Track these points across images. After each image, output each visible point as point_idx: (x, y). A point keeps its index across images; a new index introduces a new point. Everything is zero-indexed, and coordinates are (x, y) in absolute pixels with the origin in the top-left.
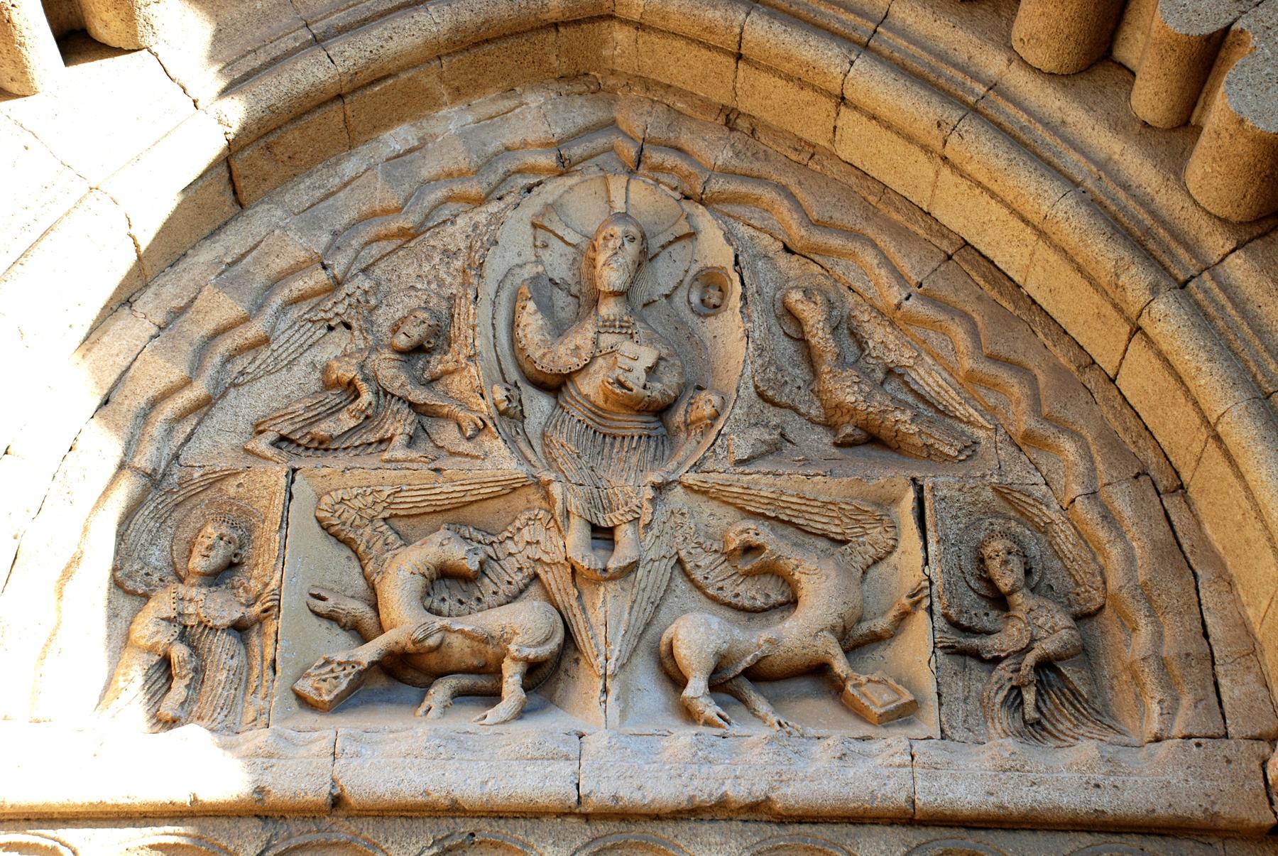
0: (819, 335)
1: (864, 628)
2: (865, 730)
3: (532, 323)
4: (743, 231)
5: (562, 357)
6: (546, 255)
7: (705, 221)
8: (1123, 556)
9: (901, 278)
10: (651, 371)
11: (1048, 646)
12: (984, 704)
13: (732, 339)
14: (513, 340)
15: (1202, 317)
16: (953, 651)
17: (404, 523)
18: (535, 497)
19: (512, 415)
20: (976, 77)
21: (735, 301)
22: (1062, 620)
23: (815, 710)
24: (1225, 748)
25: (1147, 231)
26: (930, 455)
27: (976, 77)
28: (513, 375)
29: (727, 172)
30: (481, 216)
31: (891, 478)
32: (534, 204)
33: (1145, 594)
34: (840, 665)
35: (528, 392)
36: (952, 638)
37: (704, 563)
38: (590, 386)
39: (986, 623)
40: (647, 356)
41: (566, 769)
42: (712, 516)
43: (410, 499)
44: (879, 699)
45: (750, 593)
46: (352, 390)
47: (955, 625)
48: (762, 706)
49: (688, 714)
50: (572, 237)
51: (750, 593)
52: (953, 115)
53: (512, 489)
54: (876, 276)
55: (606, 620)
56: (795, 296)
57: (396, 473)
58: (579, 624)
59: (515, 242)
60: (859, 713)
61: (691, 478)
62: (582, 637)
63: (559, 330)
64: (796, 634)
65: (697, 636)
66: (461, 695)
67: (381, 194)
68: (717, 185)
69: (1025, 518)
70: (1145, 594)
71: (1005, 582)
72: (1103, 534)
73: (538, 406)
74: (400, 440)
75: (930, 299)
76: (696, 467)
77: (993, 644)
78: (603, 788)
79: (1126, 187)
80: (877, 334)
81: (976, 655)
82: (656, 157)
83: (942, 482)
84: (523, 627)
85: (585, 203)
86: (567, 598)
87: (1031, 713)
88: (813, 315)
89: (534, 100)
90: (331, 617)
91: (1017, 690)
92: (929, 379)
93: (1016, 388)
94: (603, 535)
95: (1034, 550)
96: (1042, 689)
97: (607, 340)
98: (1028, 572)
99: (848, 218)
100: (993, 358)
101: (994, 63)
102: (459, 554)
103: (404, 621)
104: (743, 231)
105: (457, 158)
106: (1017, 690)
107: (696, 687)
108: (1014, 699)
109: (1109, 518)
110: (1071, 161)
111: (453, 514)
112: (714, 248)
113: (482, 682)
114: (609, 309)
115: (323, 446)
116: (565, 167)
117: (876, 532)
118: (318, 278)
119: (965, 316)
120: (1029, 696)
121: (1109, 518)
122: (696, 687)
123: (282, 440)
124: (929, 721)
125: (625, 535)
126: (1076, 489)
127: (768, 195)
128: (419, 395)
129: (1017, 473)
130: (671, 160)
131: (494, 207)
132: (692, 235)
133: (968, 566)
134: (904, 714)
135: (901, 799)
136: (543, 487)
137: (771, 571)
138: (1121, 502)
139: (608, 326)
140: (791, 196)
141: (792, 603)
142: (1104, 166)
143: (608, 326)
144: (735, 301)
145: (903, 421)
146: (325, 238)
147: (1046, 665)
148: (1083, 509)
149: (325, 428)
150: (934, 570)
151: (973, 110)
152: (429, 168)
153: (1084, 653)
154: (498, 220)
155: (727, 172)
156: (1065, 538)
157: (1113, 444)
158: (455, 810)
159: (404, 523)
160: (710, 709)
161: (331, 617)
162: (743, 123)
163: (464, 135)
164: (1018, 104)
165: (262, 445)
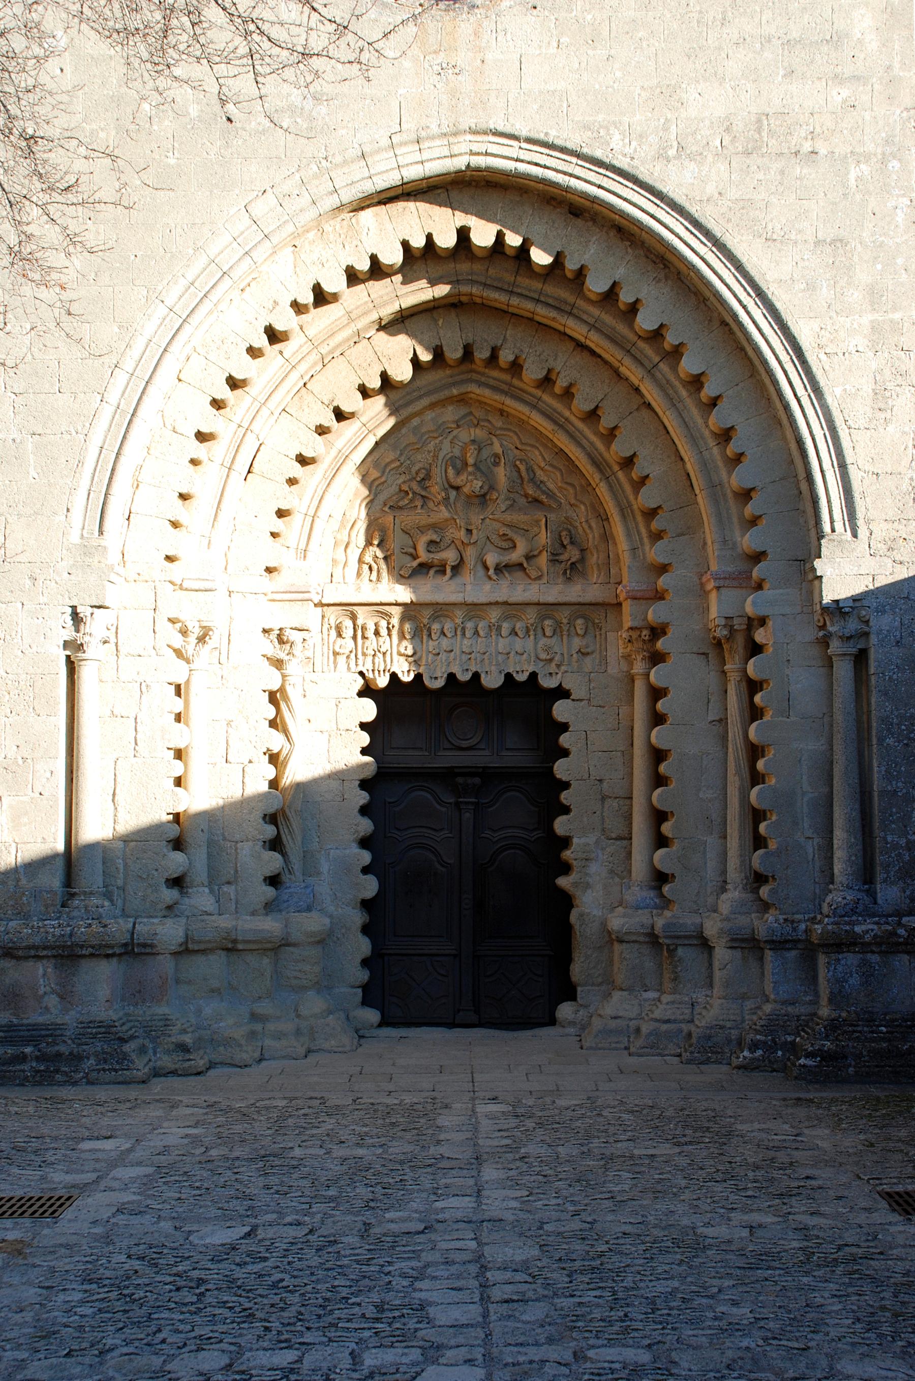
0: (524, 474)
1: (531, 554)
2: (530, 581)
3: (451, 471)
4: (505, 443)
5: (458, 482)
6: (454, 450)
7: (495, 440)
8: (592, 537)
9: (544, 459)
10: (481, 487)
11: (573, 560)
12: (558, 573)
13: (502, 474)
14: (446, 476)
15: (611, 487)
16: (551, 561)
17: (422, 529)
18: (453, 522)
19: (447, 499)
20: (562, 416)
21: (502, 464)
22: (577, 553)
23: (520, 574)
24: (609, 586)
25: (601, 463)
26: (549, 508)
27: (562, 416)
28: (447, 486)
29: (501, 429)
30: (437, 441)
31: (540, 515)
32: (450, 437)
33: (596, 547)
34: (525, 565)
35: (450, 490)
36: (551, 558)
37: (494, 537)
38: (466, 490)
39: (560, 551)
40: (480, 484)
41: (462, 595)
42: (497, 525)
43: (423, 523)
44: (534, 574)
45: (505, 545)
46: (407, 493)
47: (552, 554)
48: (507, 575)
49: (490, 578)
50: (460, 444)
51: (505, 545)
52: (556, 428)
53: (447, 520)
54: (537, 457)
55: (470, 554)
56: (518, 463)
57: (418, 517)
58: (464, 555)
59: (446, 447)
60: (530, 577)
61: (491, 517)
62: (465, 558)
63: (458, 473)
64: (516, 556)
65: (492, 559)
66: (436, 572)
67: (412, 439)
68: (498, 432)
69: (571, 524)
70: (596, 547)
71: (565, 543)
72: (588, 531)
73: (453, 494)
74: (419, 507)
75: (551, 465)
76: (492, 514)
77: (562, 558)
78: (469, 600)
79: (596, 450)
80: (539, 472)
81: (557, 561)
82: (482, 424)
83: (552, 516)
84: (450, 556)
85: (464, 435)
86: (461, 548)
87: (568, 576)
88: (522, 468)
89: (450, 408)
90: (406, 553)
91: (566, 570)
92: (551, 486)
93: (571, 491)
94: (469, 531)
95: (573, 532)
96: (571, 569)
97: (470, 478)
98: (571, 538)
99: (532, 442)
100: (566, 483)
101: (567, 413)
102: (435, 537)
103: (423, 556)
104: (505, 443)
105: (432, 427)
106: (566, 570)
107: (491, 572)
108: (565, 573)
109: (590, 527)
110: (584, 442)
111: (434, 527)
112: (497, 448)
113: (442, 569)
114: (470, 469)
115: (401, 508)
116: (458, 426)
117: (535, 529)
118: (398, 463)
119: (560, 470)
120: (568, 572)
121: (590, 527)
122: (491, 572)
123: (391, 507)
124: (545, 580)
125: (475, 532)
126: (583, 520)
127: (511, 434)
128: (423, 493)
129: (571, 513)
130: (486, 424)
131: (440, 438)
132: (492, 444)
133: (557, 537)
134: (539, 578)
135: (536, 601)
136: (455, 520)
137: (511, 540)
138: (593, 525)
139: (470, 474)
140: (517, 434)
141: (515, 547)
142: (592, 444)
143: (470, 474)
144: (502, 464)
145: (543, 498)
146: (399, 453)
147: (573, 564)
148: (584, 524)
149: (401, 504)
150: (548, 540)
151: (561, 426)
152: (424, 430)
153: (582, 560)
154: (441, 442)
155: (501, 429)
156: (580, 530)
157: (593, 506)
158: (437, 604)
159: (422, 529)
160: (495, 577)
161: (406, 553)
162: (505, 414)
163: (432, 419)
164: (573, 425)
165: (386, 509)
